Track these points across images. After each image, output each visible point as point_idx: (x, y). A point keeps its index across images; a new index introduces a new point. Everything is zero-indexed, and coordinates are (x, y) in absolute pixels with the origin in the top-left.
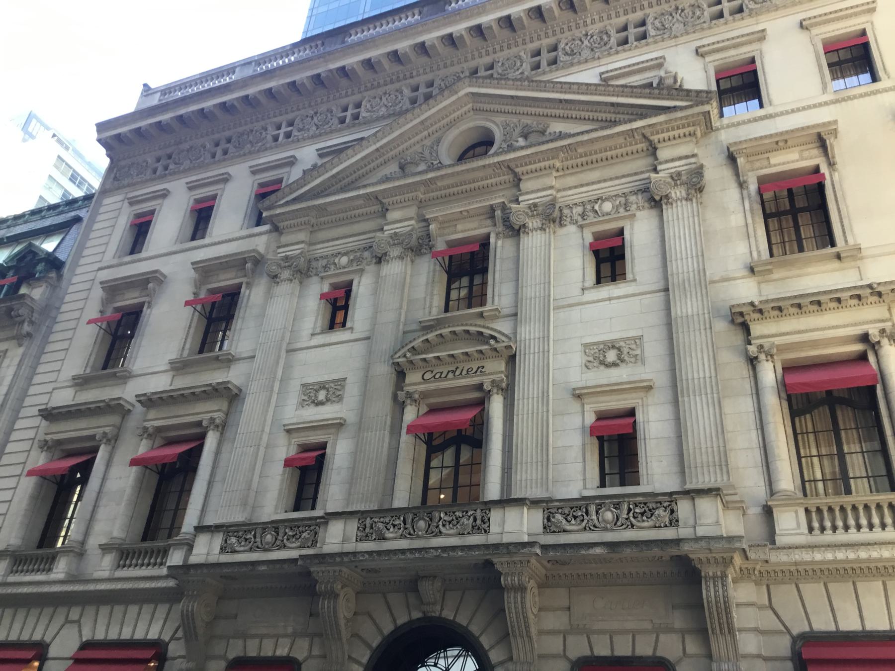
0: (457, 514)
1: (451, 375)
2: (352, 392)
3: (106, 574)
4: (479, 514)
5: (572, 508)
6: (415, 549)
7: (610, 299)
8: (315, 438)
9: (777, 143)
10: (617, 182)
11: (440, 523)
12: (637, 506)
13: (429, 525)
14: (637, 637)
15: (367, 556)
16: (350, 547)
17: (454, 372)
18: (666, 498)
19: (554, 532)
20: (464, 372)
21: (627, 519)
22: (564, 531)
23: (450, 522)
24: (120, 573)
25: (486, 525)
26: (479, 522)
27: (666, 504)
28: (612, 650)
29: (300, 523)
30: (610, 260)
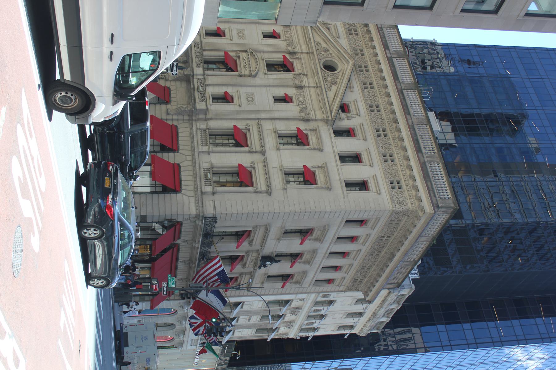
2: (242, 41)
8: (227, 34)
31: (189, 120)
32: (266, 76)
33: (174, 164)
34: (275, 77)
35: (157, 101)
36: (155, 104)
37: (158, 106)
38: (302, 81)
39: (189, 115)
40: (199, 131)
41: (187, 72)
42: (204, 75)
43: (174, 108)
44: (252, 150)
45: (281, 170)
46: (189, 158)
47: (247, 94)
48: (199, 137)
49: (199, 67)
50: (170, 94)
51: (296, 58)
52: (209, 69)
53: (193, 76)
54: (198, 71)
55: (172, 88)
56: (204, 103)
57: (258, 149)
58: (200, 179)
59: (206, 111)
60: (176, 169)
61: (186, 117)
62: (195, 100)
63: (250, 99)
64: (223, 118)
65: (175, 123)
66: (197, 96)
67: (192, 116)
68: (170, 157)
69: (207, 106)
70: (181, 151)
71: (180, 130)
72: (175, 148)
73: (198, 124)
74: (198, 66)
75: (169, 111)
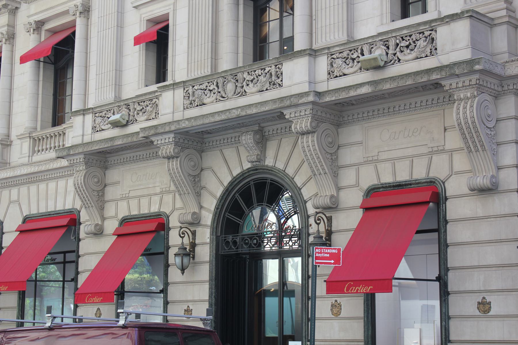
0: (257, 72)
3: (25, 160)
4: (273, 70)
5: (351, 51)
6: (222, 112)
11: (244, 83)
12: (403, 40)
13: (236, 86)
14: (415, 160)
15: (187, 122)
16: (178, 116)
19: (336, 77)
21: (395, 54)
22: (345, 75)
23: (252, 81)
24: (37, 158)
25: (279, 81)
26: (274, 78)
27: (427, 33)
28: (394, 174)
29: (144, 98)
36: (443, 247)
37: (455, 233)
39: (497, 96)
41: (302, 121)
42: (313, 53)
43: (461, 162)
50: (399, 187)
52: (287, 43)
53: (319, 94)
54: (296, 76)
56: (443, 33)
66: (408, 65)
67: (502, 79)
69: (454, 17)
74: (275, 81)
75: (482, 181)
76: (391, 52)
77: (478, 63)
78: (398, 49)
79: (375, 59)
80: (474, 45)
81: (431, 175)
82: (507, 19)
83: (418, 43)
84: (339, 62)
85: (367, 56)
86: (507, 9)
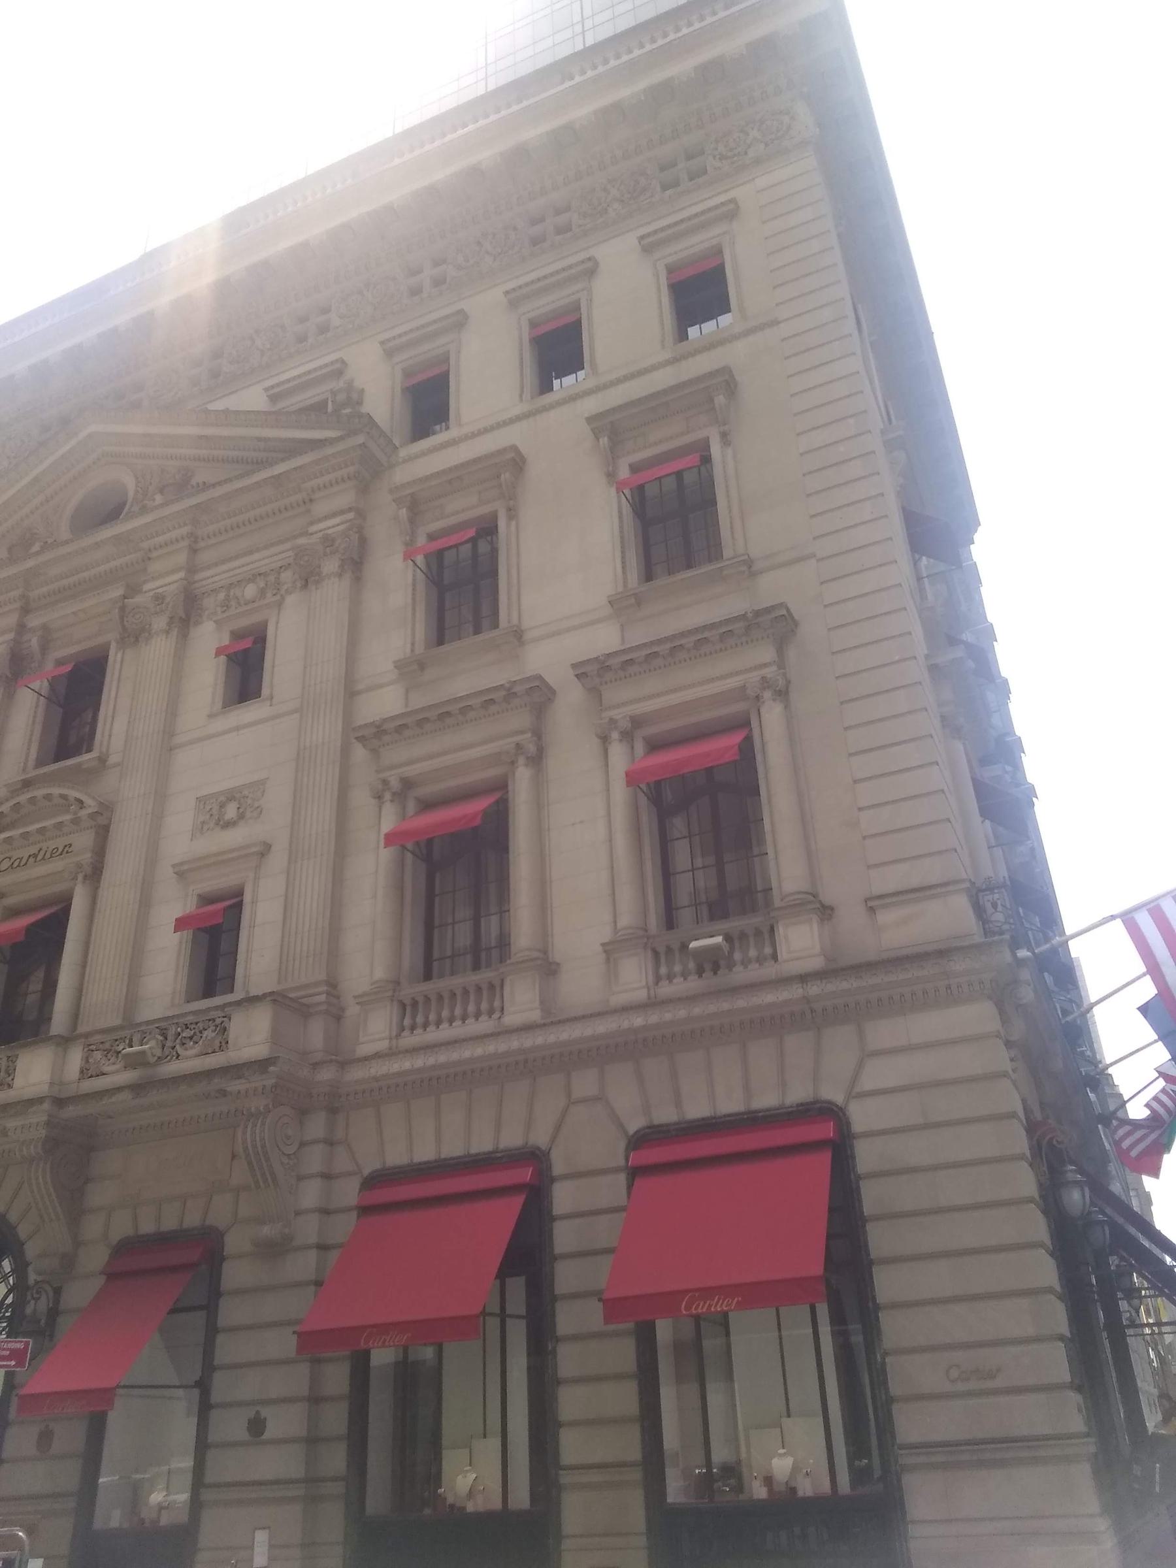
1: (32, 860)
7: (237, 729)
9: (450, 482)
10: (266, 553)
17: (35, 856)
18: (221, 1014)
20: (48, 855)
30: (246, 672)
31: (333, 1111)
32: (113, 759)
33: (635, 1173)
34: (120, 726)
35: (199, 1318)
37: (231, 1312)
38: (159, 599)
40: (409, 1040)
44: (532, 748)
45: (639, 600)
46: (585, 1083)
47: (200, 829)
48: (446, 1032)
49: (10, 1072)
51: (44, 648)
55: (122, 1227)
57: (519, 719)
58: (735, 990)
59: (286, 1003)
60: (662, 1154)
61: (316, 1126)
62: (209, 1074)
63: (228, 807)
64: (333, 911)
65: (349, 1193)
66: (190, 1061)
68: (588, 1205)
70: (540, 1138)
71: (396, 1157)
72: (526, 1174)
73: (364, 1050)
76: (169, 1044)
77: (274, 1064)
78: (178, 1041)
79: (143, 1053)
80: (276, 1037)
81: (208, 1223)
82: (324, 1007)
83: (205, 1033)
84: (98, 1055)
85: (136, 1049)
86: (328, 994)
